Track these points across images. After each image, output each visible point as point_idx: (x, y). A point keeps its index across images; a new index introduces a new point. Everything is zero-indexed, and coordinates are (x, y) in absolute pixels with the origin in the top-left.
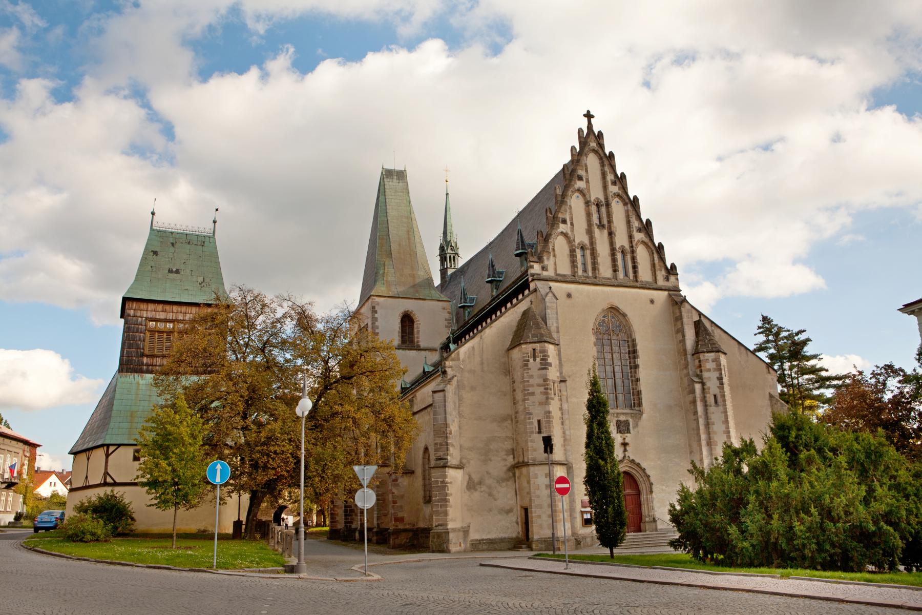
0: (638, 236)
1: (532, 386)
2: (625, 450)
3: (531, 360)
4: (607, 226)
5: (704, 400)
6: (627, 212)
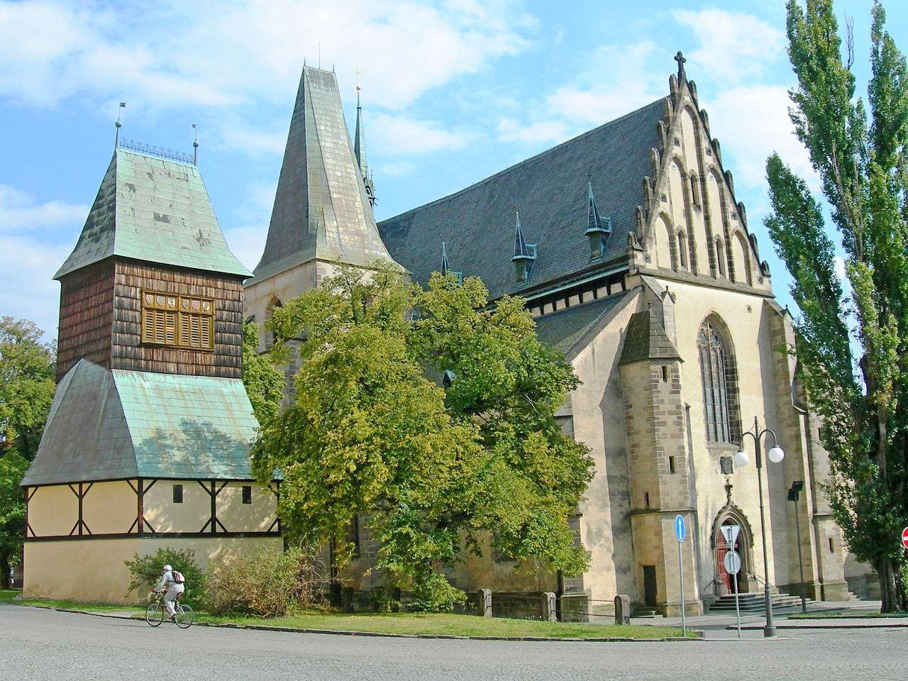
1: (663, 413)
2: (729, 495)
5: (808, 435)
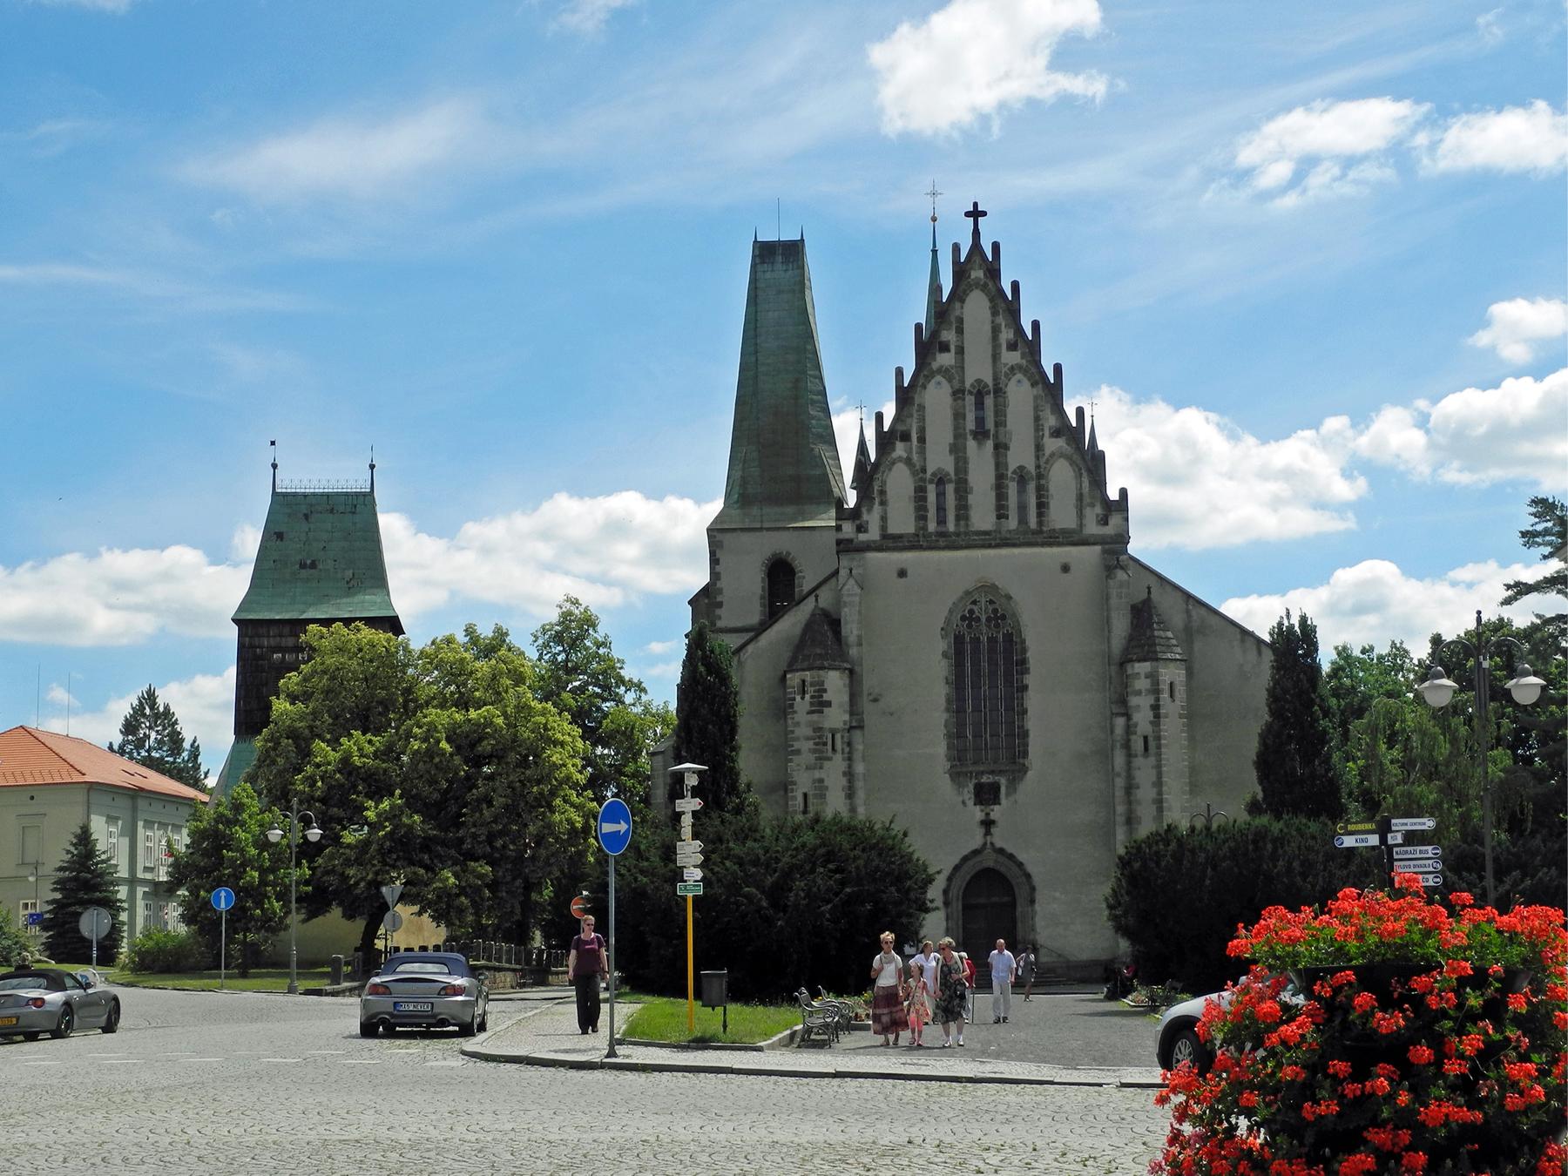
0: (1052, 444)
2: (988, 833)
3: (798, 698)
4: (989, 431)
6: (1036, 398)
